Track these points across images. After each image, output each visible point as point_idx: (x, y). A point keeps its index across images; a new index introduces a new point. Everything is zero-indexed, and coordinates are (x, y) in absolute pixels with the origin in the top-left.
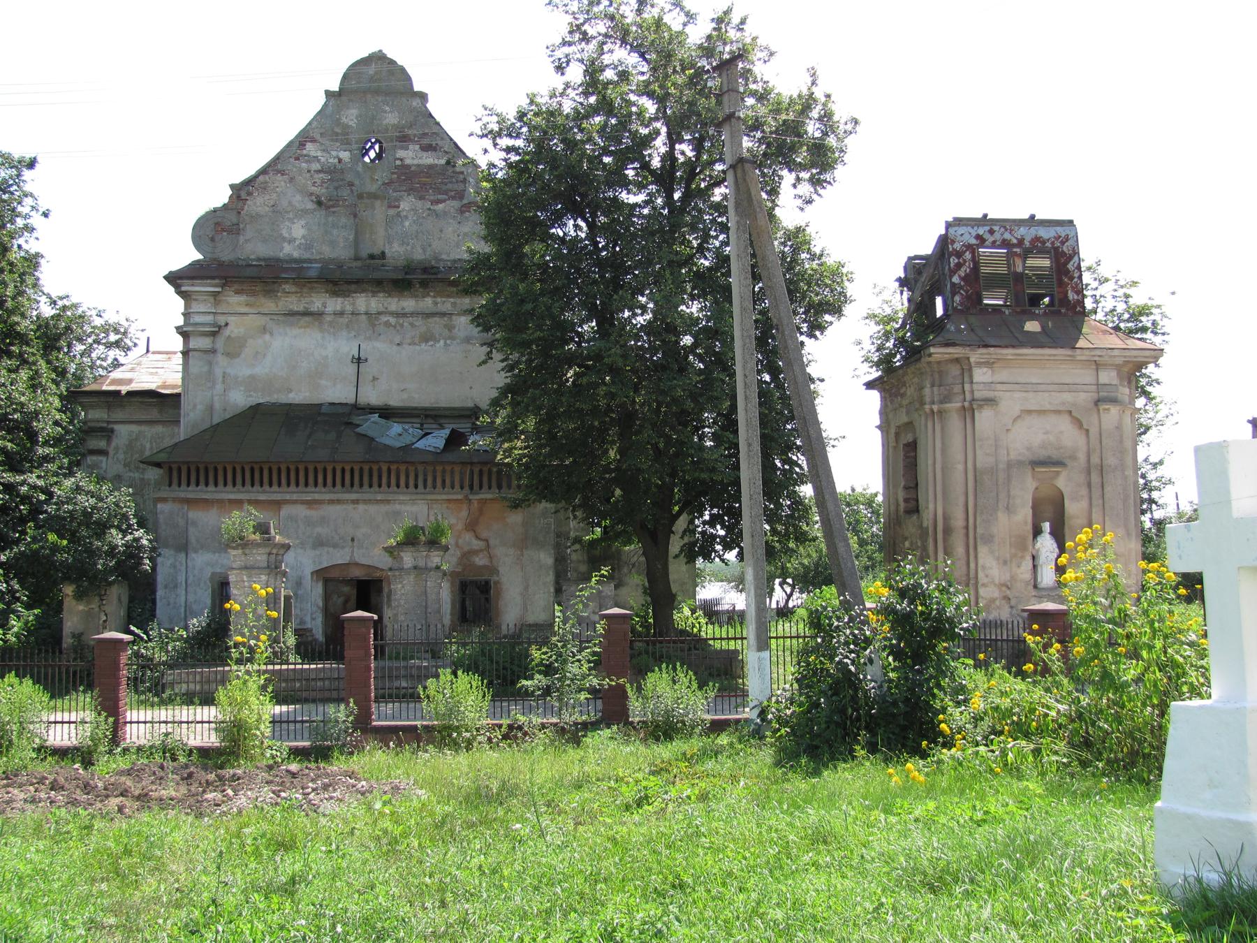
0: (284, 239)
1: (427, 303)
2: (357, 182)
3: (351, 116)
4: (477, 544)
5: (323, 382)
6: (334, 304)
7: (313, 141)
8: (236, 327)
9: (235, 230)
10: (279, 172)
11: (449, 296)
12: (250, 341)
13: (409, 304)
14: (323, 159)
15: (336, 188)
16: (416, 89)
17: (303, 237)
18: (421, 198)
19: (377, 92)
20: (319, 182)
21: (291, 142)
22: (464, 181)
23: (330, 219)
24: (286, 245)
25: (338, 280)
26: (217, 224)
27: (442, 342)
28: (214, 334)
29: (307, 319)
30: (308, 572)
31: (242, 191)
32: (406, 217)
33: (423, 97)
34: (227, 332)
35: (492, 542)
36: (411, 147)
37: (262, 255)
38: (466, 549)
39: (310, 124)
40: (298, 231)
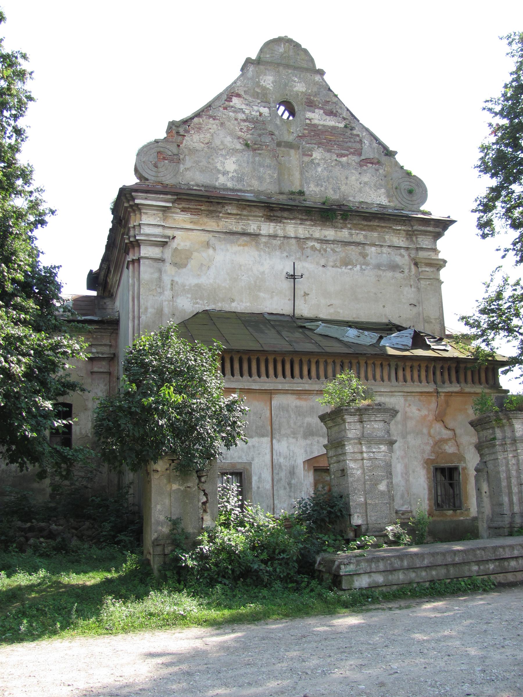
0: (219, 171)
1: (344, 234)
2: (276, 133)
3: (268, 81)
4: (446, 434)
5: (262, 295)
6: (267, 228)
7: (238, 96)
8: (182, 241)
9: (176, 159)
10: (210, 117)
11: (361, 229)
12: (195, 254)
13: (330, 233)
14: (247, 112)
15: (260, 135)
16: (318, 67)
17: (235, 171)
18: (329, 151)
19: (287, 66)
20: (245, 129)
21: (221, 94)
22: (361, 142)
23: (257, 159)
24: (220, 176)
25: (274, 209)
26: (158, 153)
27: (358, 267)
28: (164, 244)
29: (245, 238)
30: (300, 459)
31: (177, 129)
32: (318, 164)
33: (321, 73)
34: (174, 244)
35: (458, 431)
36: (317, 111)
37: (200, 183)
38: (437, 438)
39: (235, 82)
40: (230, 165)
